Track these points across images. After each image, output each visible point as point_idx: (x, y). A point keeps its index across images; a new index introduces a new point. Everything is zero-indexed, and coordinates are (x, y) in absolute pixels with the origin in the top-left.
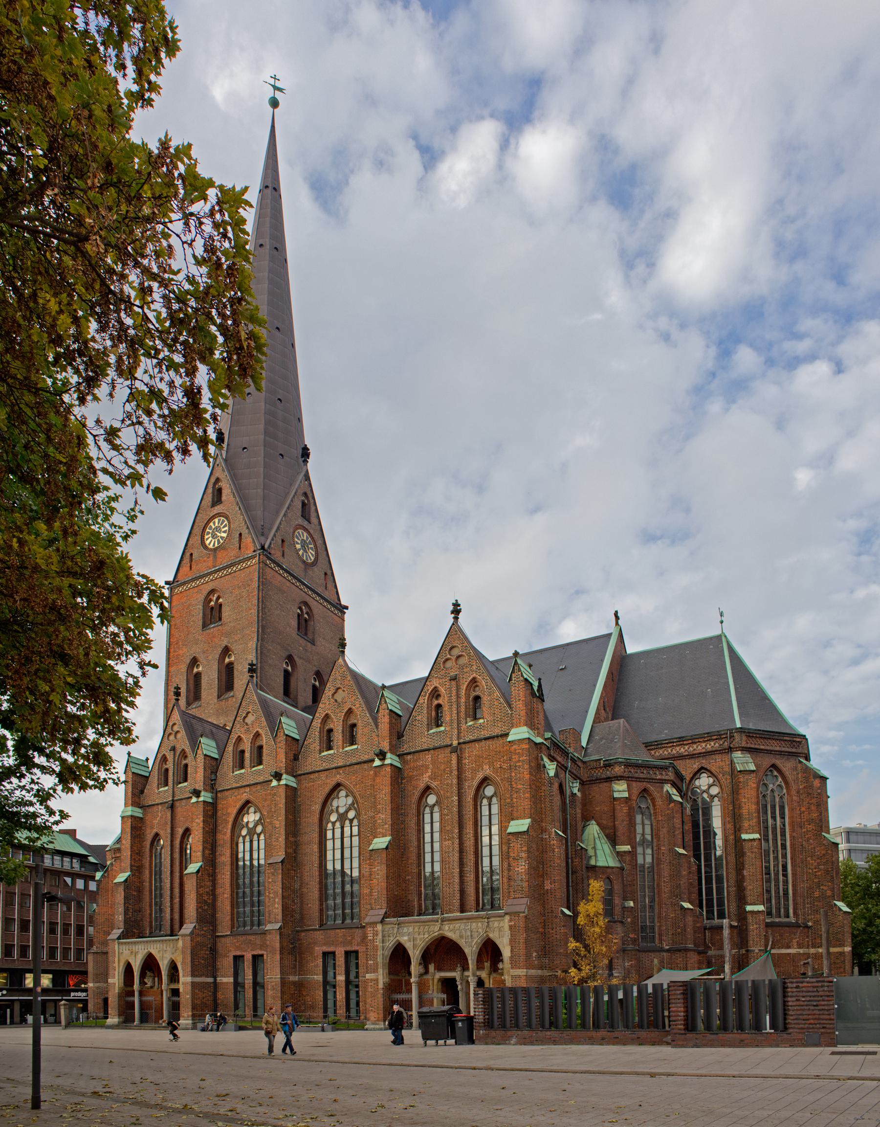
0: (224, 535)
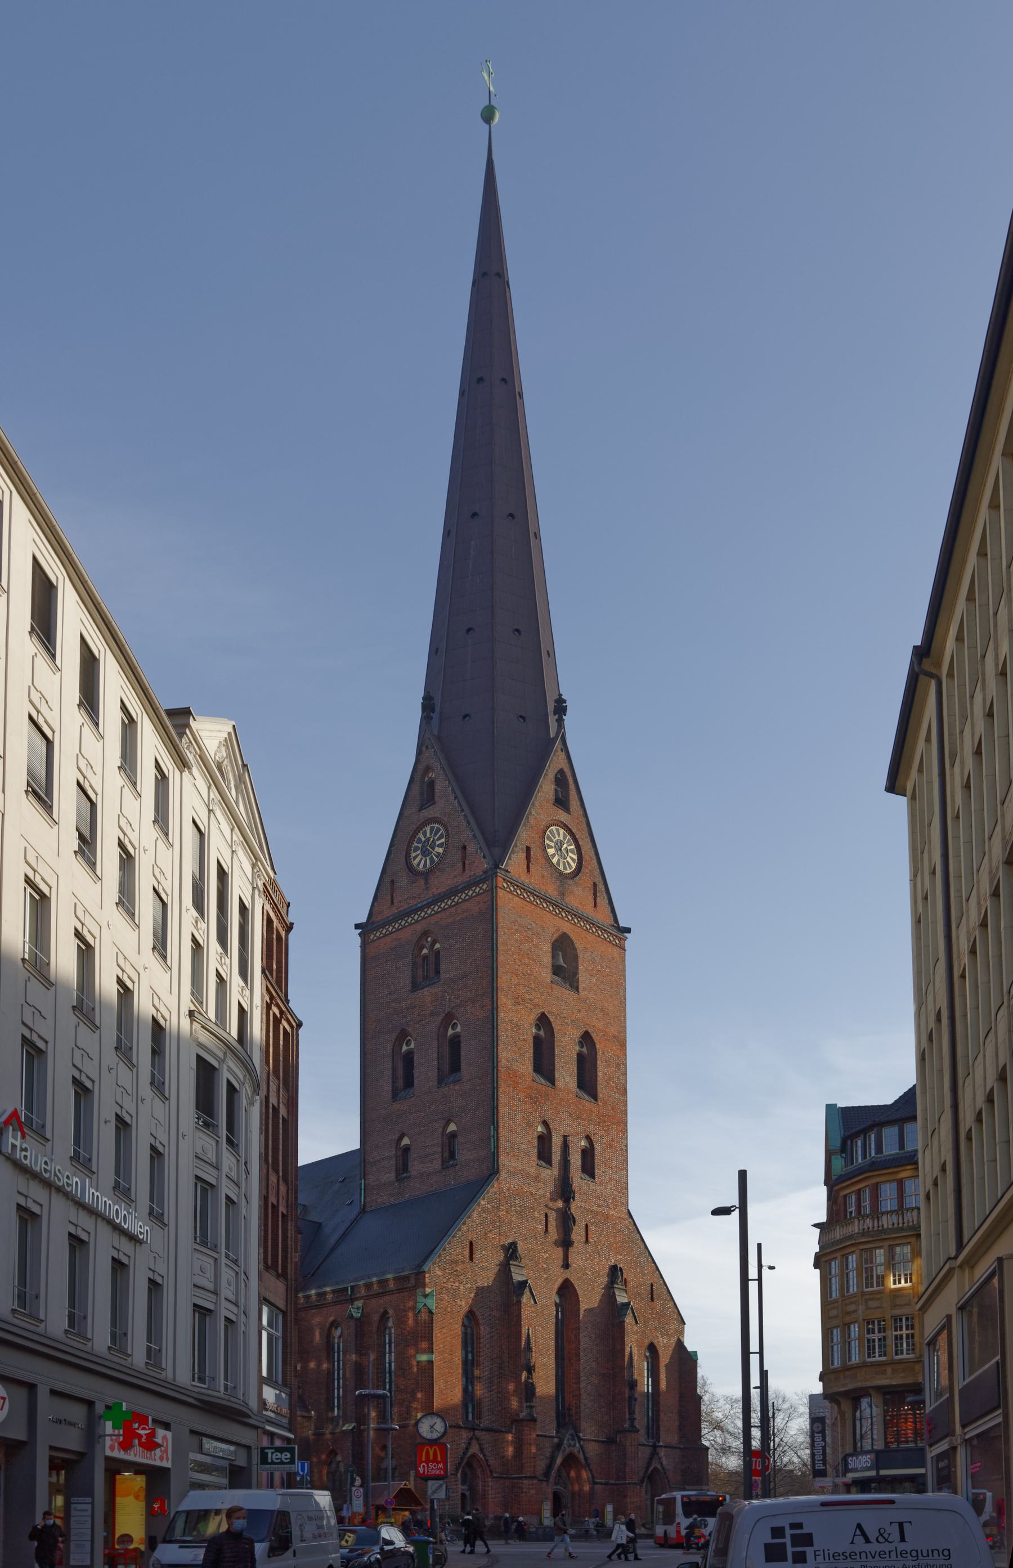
0: (440, 850)
